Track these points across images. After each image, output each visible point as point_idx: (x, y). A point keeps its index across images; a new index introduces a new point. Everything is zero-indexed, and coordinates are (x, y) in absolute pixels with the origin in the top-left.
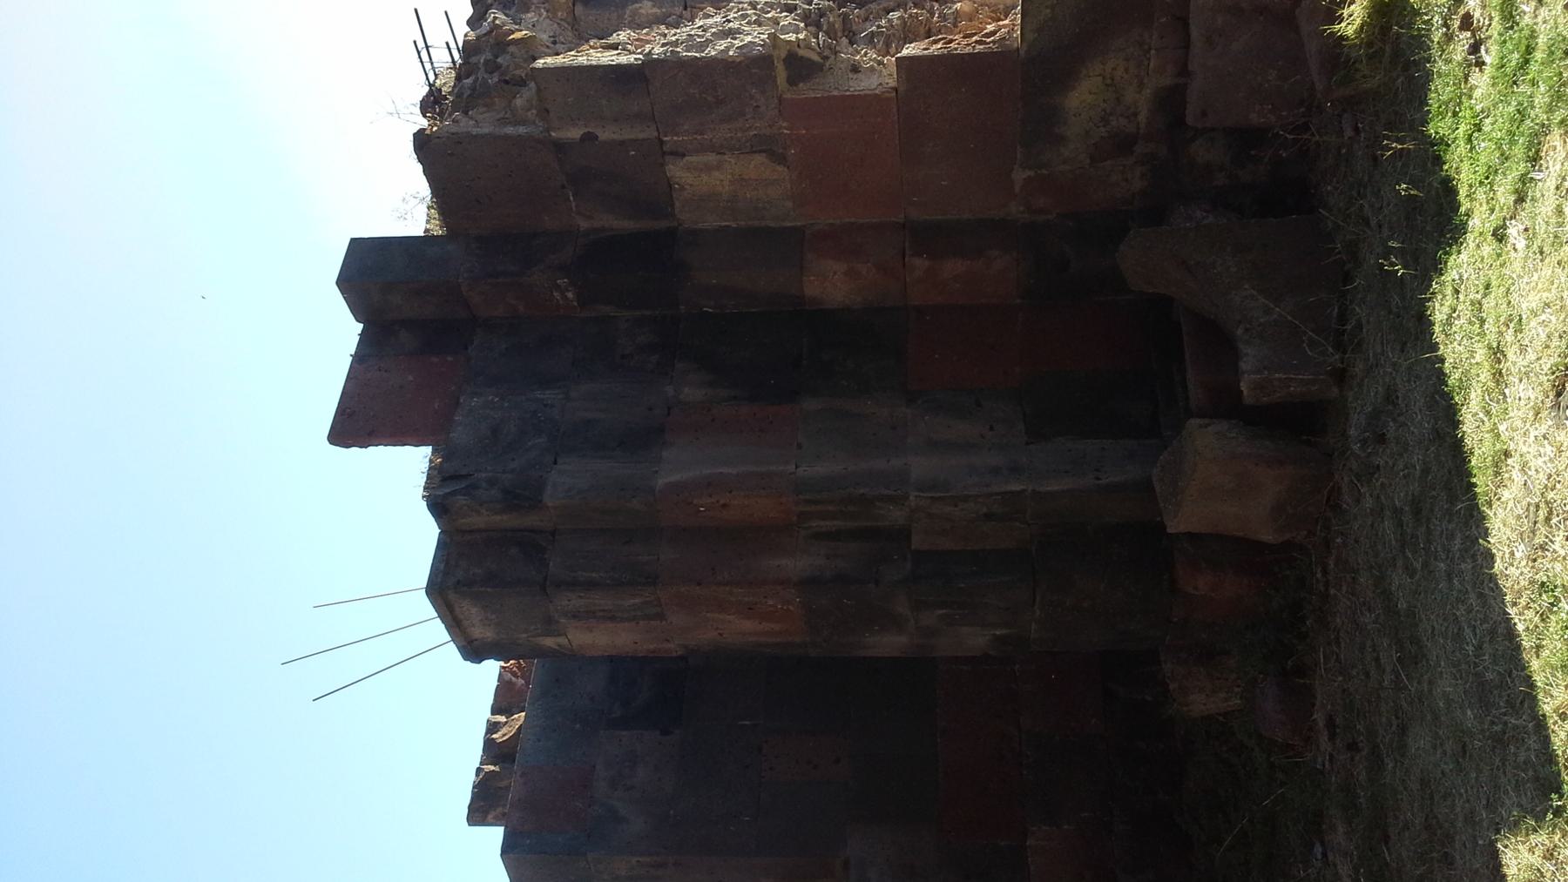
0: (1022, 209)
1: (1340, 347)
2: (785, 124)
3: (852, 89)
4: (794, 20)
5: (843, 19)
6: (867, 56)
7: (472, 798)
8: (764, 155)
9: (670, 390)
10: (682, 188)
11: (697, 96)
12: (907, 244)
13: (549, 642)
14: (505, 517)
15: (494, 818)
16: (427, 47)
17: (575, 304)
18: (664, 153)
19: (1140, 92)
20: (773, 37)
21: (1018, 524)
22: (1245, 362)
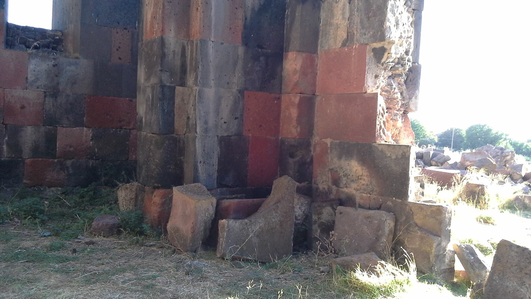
0: (316, 141)
1: (234, 259)
2: (357, 46)
3: (368, 74)
4: (401, 54)
5: (400, 74)
8: (346, 37)
11: (372, 8)
12: (306, 95)
19: (354, 189)
20: (393, 43)
21: (185, 130)
22: (233, 222)
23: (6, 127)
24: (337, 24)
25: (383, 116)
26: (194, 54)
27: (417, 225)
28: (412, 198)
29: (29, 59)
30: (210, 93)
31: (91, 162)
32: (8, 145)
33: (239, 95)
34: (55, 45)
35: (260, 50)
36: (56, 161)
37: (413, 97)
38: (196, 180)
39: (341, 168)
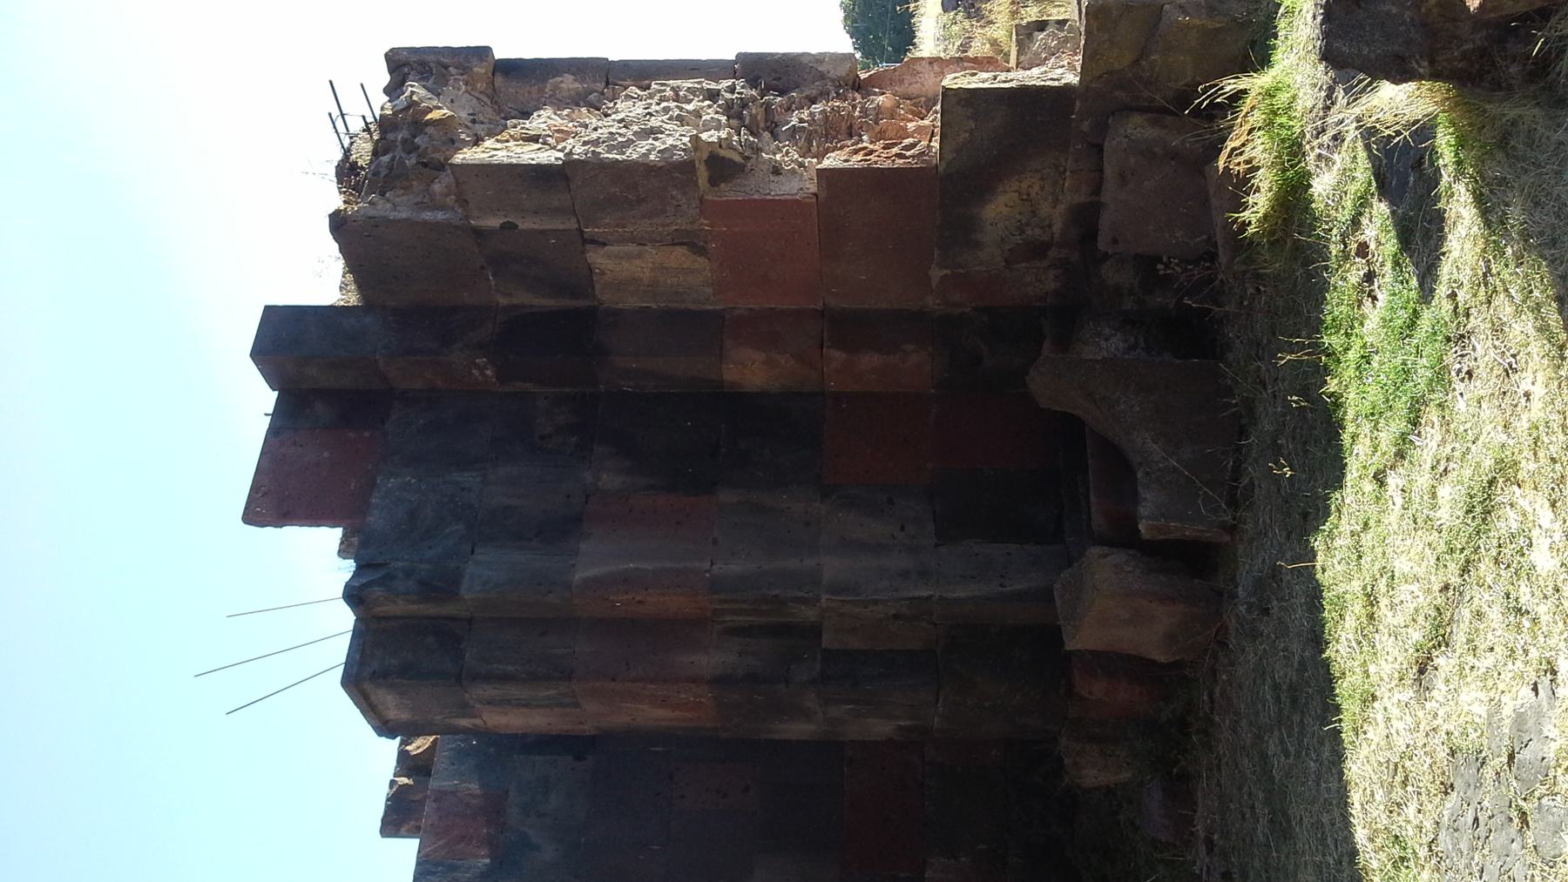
0: (938, 302)
1: (1233, 503)
2: (705, 222)
3: (772, 193)
4: (717, 112)
5: (766, 110)
6: (787, 155)
7: (386, 812)
8: (685, 247)
9: (588, 477)
10: (603, 273)
13: (465, 722)
14: (421, 606)
16: (343, 115)
17: (494, 380)
18: (585, 241)
19: (1054, 207)
20: (695, 139)
22: (1143, 506)
24: (652, 270)
25: (871, 152)
26: (744, 606)
27: (1137, 62)
28: (1072, 79)
30: (833, 567)
33: (834, 497)
35: (723, 450)
37: (819, 69)
38: (1047, 596)
39: (1002, 240)
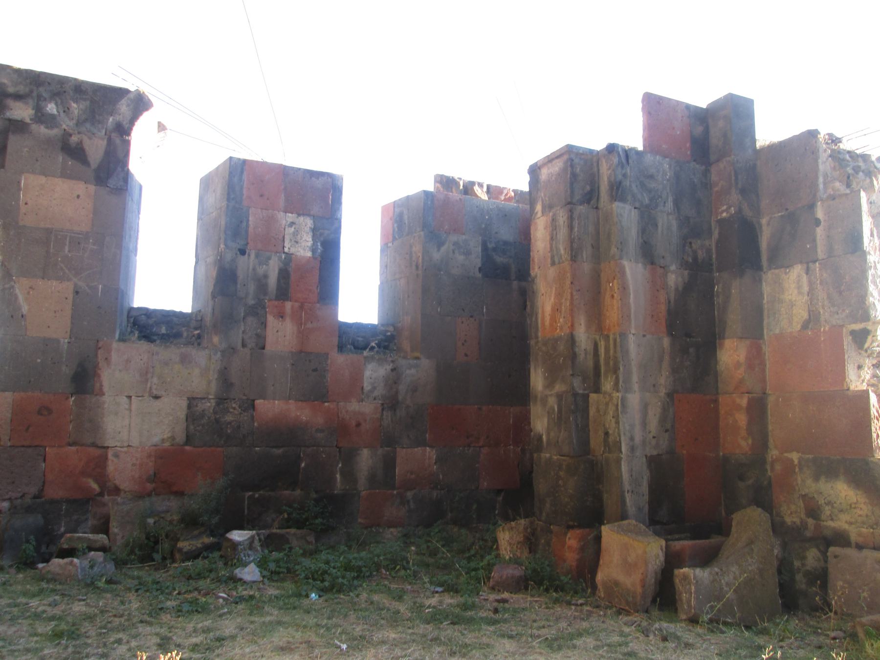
0: (774, 457)
1: (711, 621)
2: (827, 329)
7: (447, 176)
8: (808, 318)
9: (673, 268)
10: (786, 273)
11: (844, 280)
13: (539, 208)
14: (606, 183)
15: (438, 188)
17: (719, 218)
18: (808, 263)
19: (846, 522)
21: (603, 449)
23: (340, 452)
24: (790, 300)
26: (612, 352)
29: (365, 364)
30: (634, 399)
31: (435, 494)
32: (342, 474)
33: (668, 400)
34: (386, 344)
35: (688, 340)
36: (395, 492)
38: (624, 516)
39: (821, 493)
